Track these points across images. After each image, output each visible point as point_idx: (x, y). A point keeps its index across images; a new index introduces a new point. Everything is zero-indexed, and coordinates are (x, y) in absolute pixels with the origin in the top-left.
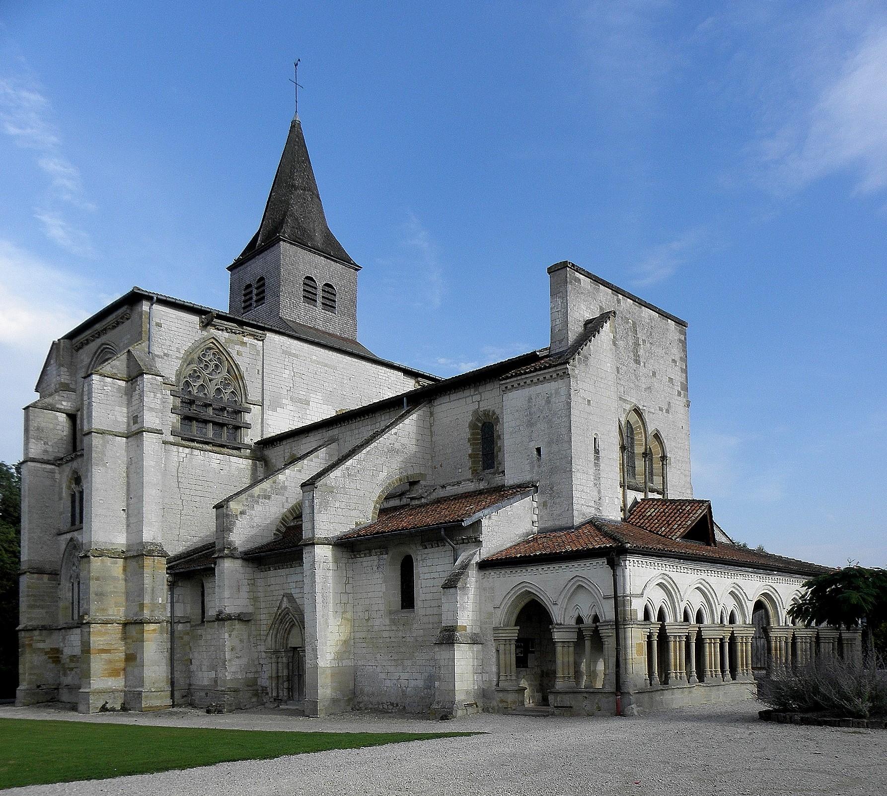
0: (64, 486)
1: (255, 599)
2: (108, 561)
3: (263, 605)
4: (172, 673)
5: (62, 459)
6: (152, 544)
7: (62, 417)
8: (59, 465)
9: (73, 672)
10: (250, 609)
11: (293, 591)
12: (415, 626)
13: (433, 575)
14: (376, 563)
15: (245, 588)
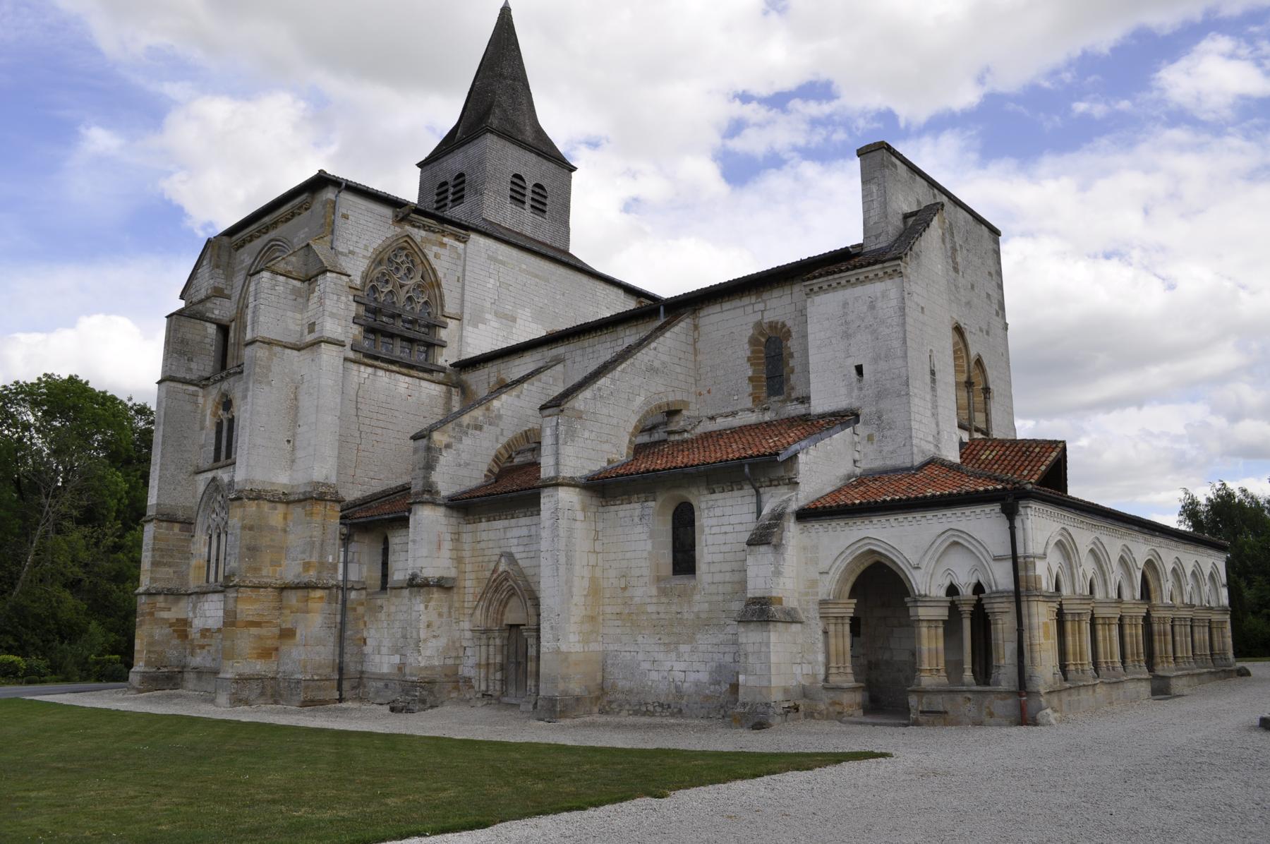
0: (209, 412)
1: (459, 560)
2: (266, 506)
3: (468, 568)
4: (341, 654)
5: (208, 379)
6: (324, 484)
7: (212, 329)
8: (204, 387)
9: (205, 651)
10: (452, 573)
11: (514, 550)
12: (697, 598)
13: (724, 529)
14: (637, 512)
15: (447, 545)
